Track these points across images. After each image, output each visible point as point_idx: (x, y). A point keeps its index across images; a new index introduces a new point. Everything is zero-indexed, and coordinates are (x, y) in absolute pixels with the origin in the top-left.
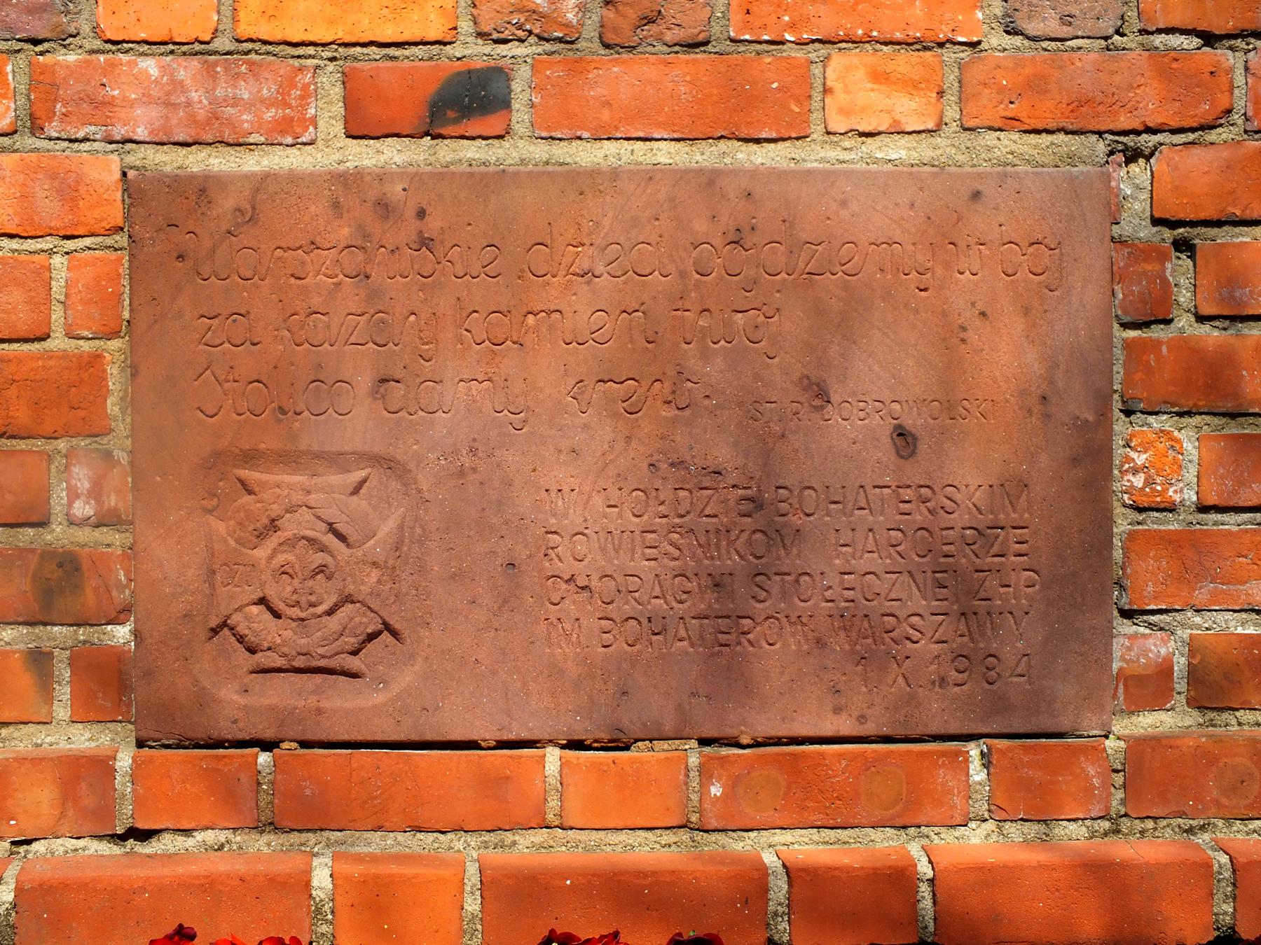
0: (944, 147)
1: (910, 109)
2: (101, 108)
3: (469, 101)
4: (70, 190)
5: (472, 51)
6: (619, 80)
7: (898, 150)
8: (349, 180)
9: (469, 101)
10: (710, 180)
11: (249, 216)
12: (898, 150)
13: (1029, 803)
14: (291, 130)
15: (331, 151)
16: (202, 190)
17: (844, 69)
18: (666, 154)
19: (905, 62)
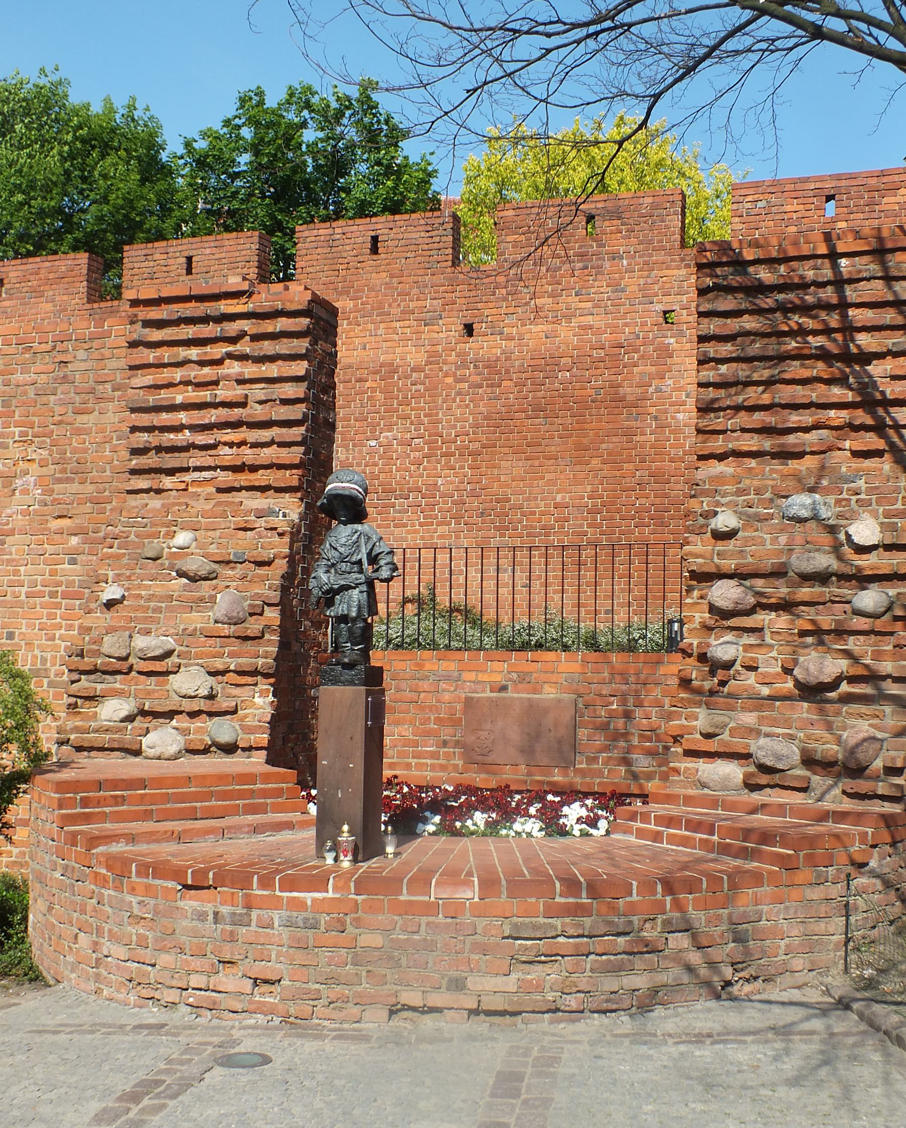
0: (558, 696)
1: (554, 691)
2: (463, 689)
3: (504, 688)
4: (459, 698)
5: (504, 682)
6: (520, 686)
7: (552, 696)
8: (489, 698)
9: (504, 688)
10: (529, 699)
11: (477, 701)
12: (552, 696)
13: (566, 775)
14: (484, 691)
15: (488, 694)
16: (472, 698)
17: (545, 686)
18: (525, 695)
19: (553, 685)
